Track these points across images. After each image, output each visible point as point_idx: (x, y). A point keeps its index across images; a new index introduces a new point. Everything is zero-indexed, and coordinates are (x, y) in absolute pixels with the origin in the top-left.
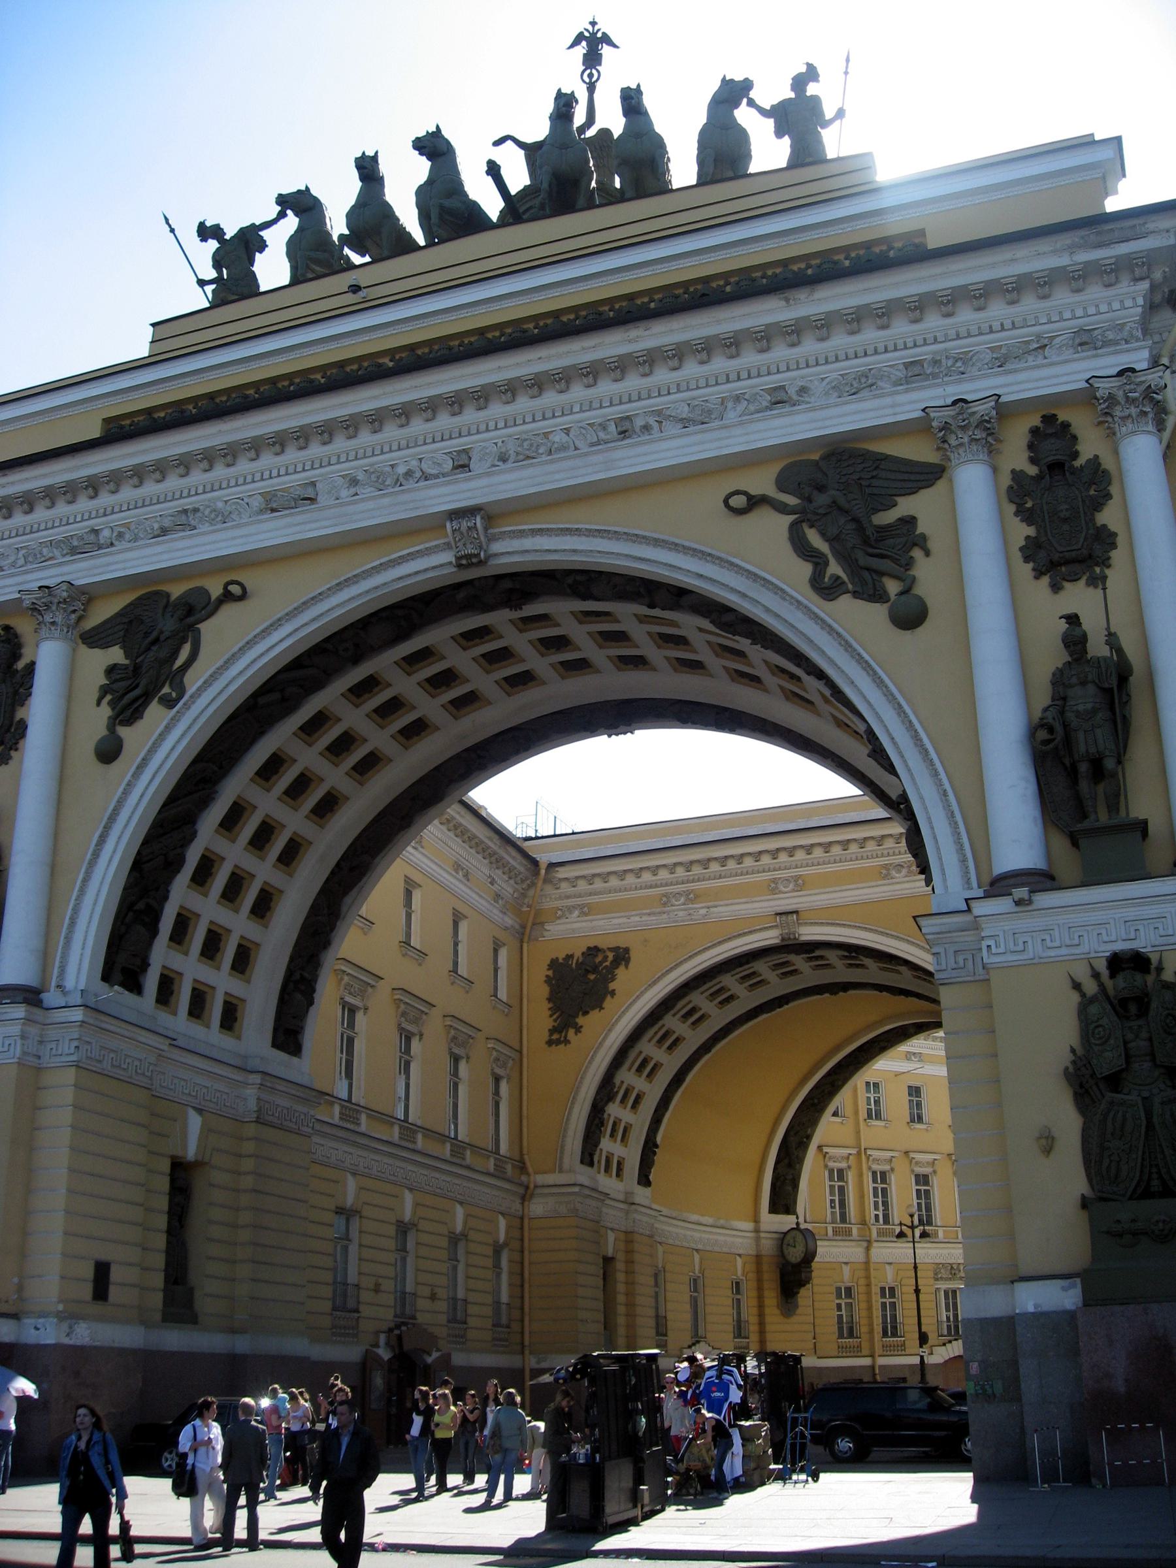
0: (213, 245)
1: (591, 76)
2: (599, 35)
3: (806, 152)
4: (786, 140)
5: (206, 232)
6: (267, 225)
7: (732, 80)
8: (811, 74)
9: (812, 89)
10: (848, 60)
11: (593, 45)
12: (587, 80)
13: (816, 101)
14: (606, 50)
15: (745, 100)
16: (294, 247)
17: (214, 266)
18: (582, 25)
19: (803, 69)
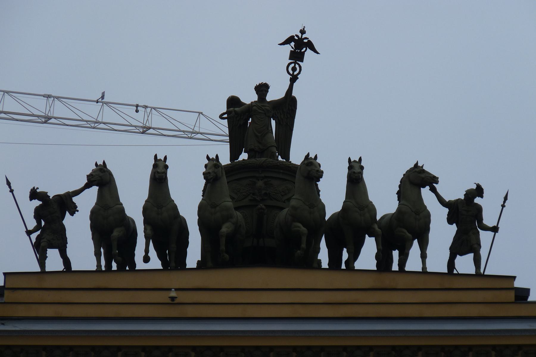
0: (37, 203)
1: (294, 69)
2: (306, 41)
3: (466, 242)
4: (454, 228)
5: (34, 194)
6: (77, 193)
7: (424, 171)
8: (479, 191)
9: (477, 200)
10: (506, 198)
11: (299, 47)
12: (291, 72)
13: (479, 209)
14: (309, 53)
15: (428, 188)
16: (95, 215)
17: (35, 217)
18: (296, 32)
19: (475, 187)
